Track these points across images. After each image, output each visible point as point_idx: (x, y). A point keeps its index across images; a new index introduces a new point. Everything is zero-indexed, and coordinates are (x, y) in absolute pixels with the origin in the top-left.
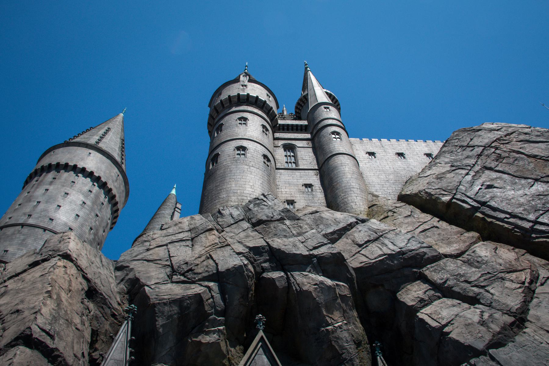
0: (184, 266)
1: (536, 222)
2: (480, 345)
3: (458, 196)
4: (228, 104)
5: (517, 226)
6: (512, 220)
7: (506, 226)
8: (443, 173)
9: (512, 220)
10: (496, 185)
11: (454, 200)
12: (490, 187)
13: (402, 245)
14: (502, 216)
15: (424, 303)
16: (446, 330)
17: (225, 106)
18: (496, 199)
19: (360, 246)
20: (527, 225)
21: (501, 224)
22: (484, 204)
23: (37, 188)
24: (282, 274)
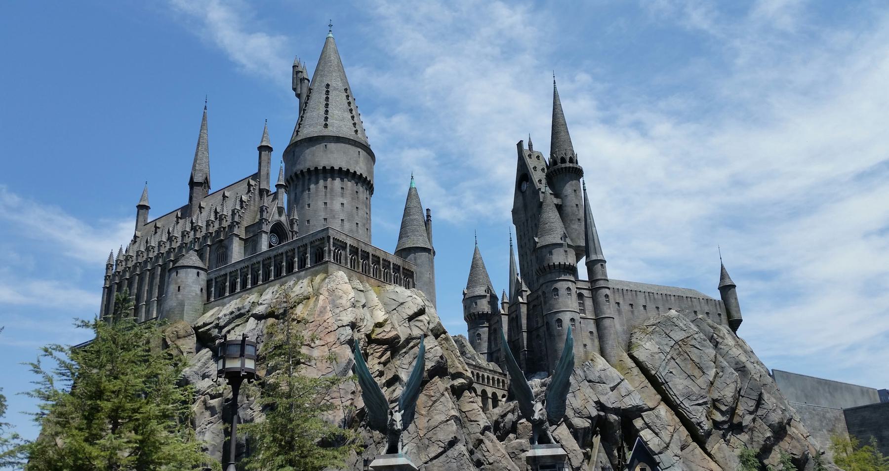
0: (577, 410)
1: (682, 402)
2: (657, 452)
3: (658, 373)
4: (558, 268)
5: (675, 401)
6: (674, 397)
7: (672, 398)
8: (654, 353)
9: (674, 397)
10: (674, 373)
11: (656, 375)
12: (671, 372)
13: (638, 402)
14: (672, 393)
15: (642, 429)
16: (648, 443)
17: (556, 268)
18: (672, 383)
19: (623, 397)
20: (679, 402)
21: (670, 397)
22: (667, 382)
23: (332, 199)
24: (604, 414)
